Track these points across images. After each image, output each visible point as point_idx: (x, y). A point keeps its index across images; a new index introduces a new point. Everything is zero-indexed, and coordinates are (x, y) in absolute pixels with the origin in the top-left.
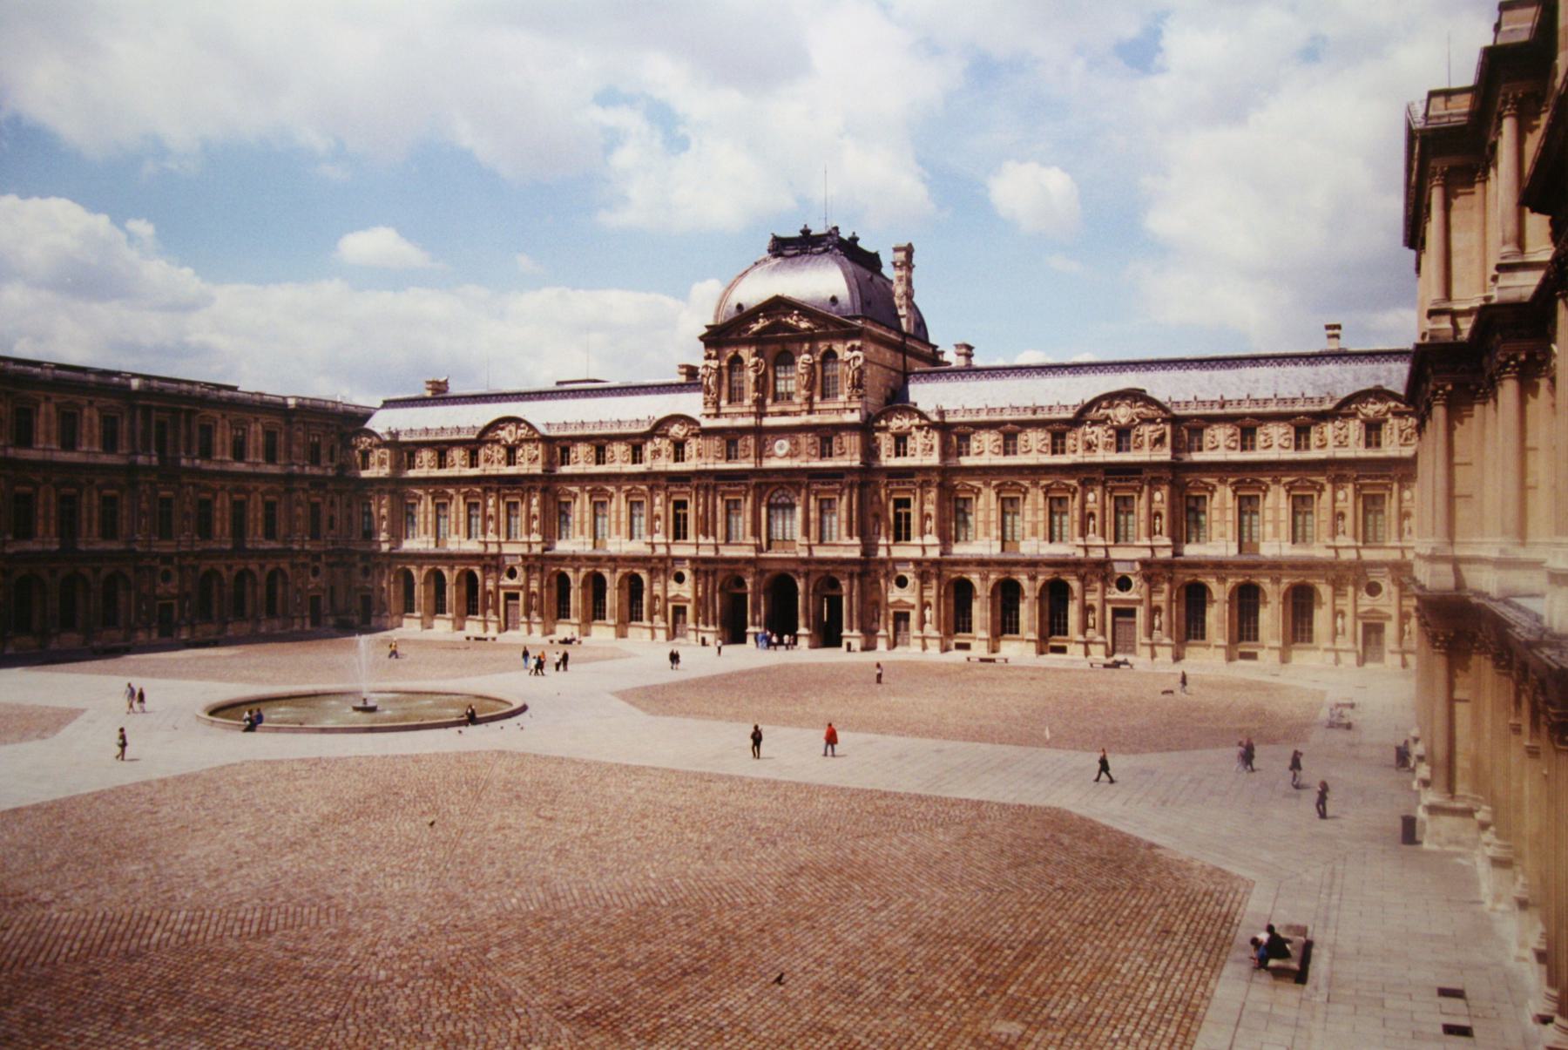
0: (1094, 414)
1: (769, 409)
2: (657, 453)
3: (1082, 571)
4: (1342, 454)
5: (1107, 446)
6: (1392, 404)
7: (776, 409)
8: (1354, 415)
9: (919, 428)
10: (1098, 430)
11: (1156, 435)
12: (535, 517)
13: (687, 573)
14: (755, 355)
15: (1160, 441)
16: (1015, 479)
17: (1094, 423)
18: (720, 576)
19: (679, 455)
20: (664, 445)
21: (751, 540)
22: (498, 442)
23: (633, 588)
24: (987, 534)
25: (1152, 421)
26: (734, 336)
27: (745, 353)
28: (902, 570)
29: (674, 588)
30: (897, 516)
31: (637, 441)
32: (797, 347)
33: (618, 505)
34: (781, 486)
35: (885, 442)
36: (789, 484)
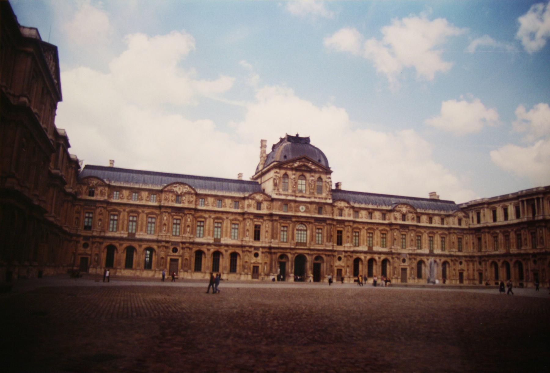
0: (397, 209)
1: (297, 195)
2: (249, 206)
3: (394, 256)
5: (400, 219)
6: (464, 214)
7: (300, 195)
9: (347, 207)
12: (188, 226)
14: (294, 174)
15: (413, 219)
16: (372, 226)
17: (397, 211)
18: (279, 254)
20: (252, 202)
21: (292, 242)
22: (173, 192)
24: (364, 244)
25: (411, 213)
26: (285, 166)
27: (289, 173)
29: (254, 260)
31: (237, 200)
34: (302, 223)
35: (336, 211)
36: (306, 222)
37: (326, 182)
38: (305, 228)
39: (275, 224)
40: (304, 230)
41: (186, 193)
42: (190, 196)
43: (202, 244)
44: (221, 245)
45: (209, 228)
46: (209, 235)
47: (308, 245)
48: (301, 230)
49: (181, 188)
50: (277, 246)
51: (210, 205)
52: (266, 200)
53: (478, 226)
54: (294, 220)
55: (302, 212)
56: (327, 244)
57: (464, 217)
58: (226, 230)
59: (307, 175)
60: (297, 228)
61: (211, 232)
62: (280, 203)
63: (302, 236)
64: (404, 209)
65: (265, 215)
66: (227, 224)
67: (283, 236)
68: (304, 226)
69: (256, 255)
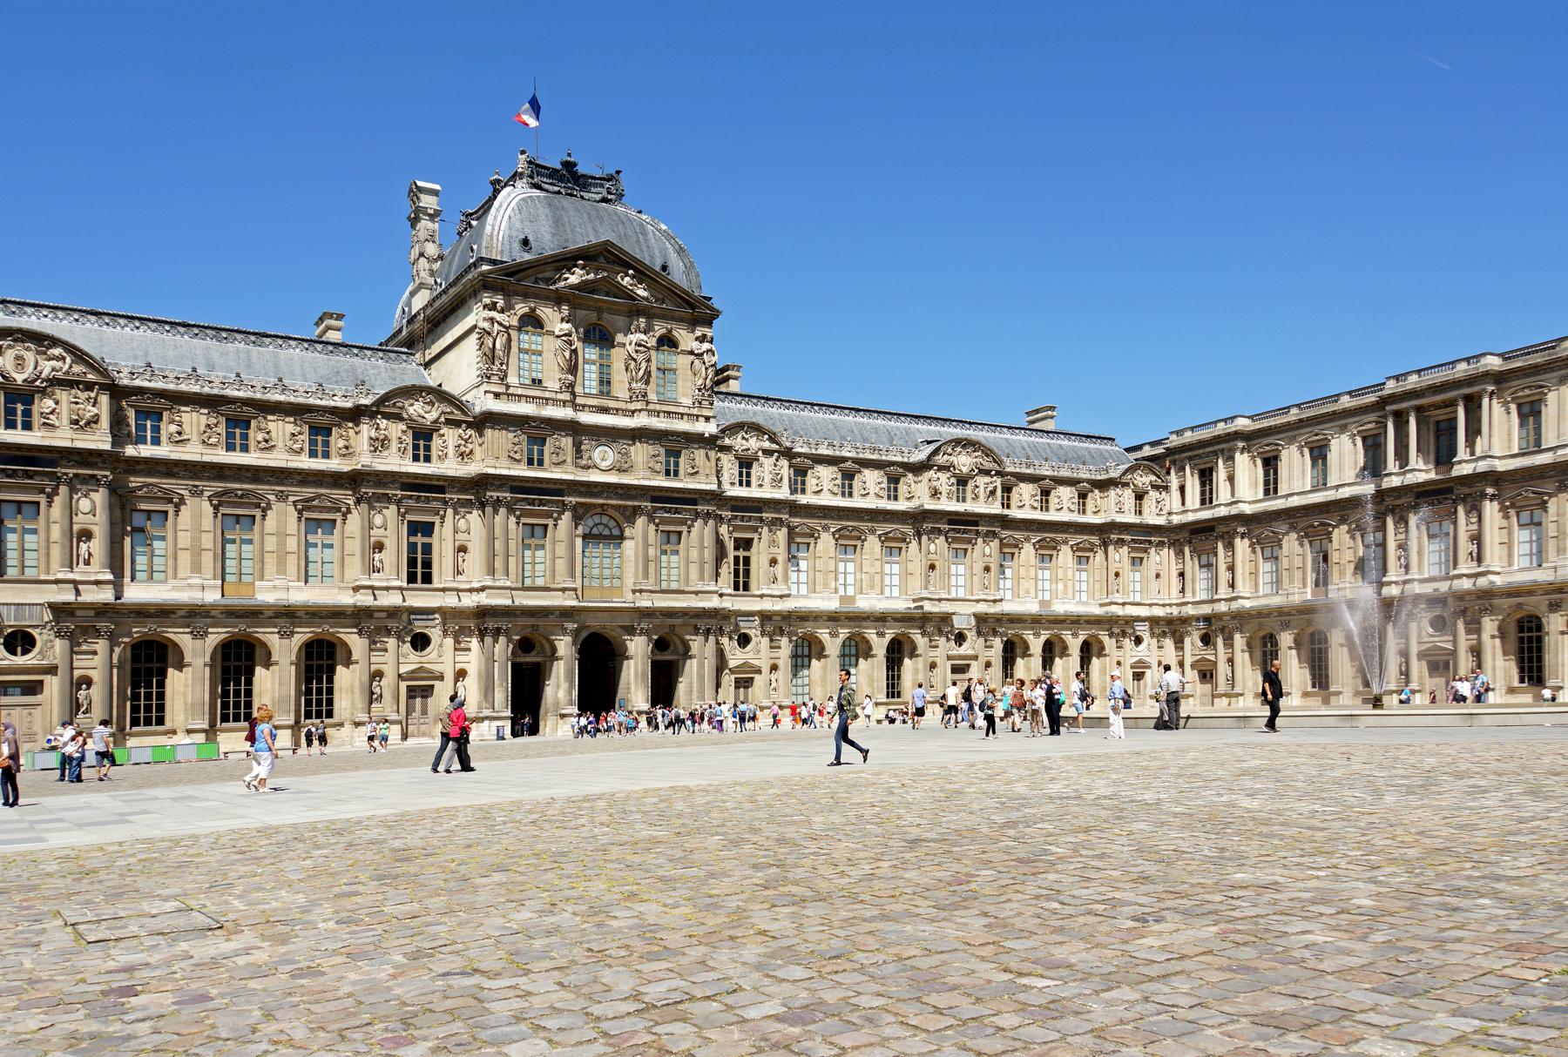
2: (379, 444)
4: (1120, 519)
6: (1154, 478)
8: (1127, 485)
10: (943, 476)
11: (991, 487)
13: (435, 634)
15: (993, 492)
17: (941, 468)
19: (421, 451)
20: (395, 430)
23: (319, 662)
24: (826, 585)
25: (987, 473)
27: (548, 314)
28: (745, 627)
30: (736, 559)
31: (324, 420)
32: (621, 321)
33: (281, 519)
37: (691, 353)
41: (55, 382)
42: (83, 395)
43: (164, 612)
44: (255, 614)
45: (196, 540)
46: (197, 568)
49: (30, 357)
51: (191, 438)
52: (449, 422)
53: (1206, 514)
57: (1155, 487)
58: (281, 544)
61: (208, 560)
64: (964, 461)
66: (282, 523)
68: (612, 523)
69: (421, 642)
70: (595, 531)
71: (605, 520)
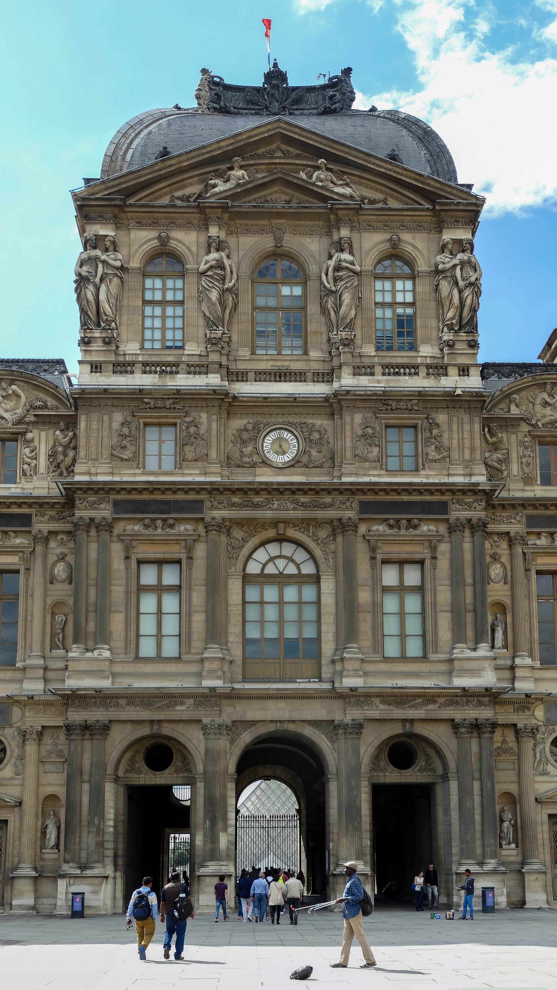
1: (241, 366)
21: (214, 652)
27: (186, 240)
36: (305, 524)
38: (308, 569)
39: (93, 551)
40: (299, 579)
47: (326, 672)
48: (281, 580)
50: (105, 684)
52: (43, 421)
54: (218, 514)
55: (280, 469)
56: (462, 651)
59: (311, 246)
60: (253, 568)
62: (118, 417)
63: (291, 613)
65: (40, 504)
67: (160, 619)
68: (300, 556)
70: (270, 569)
71: (288, 549)
